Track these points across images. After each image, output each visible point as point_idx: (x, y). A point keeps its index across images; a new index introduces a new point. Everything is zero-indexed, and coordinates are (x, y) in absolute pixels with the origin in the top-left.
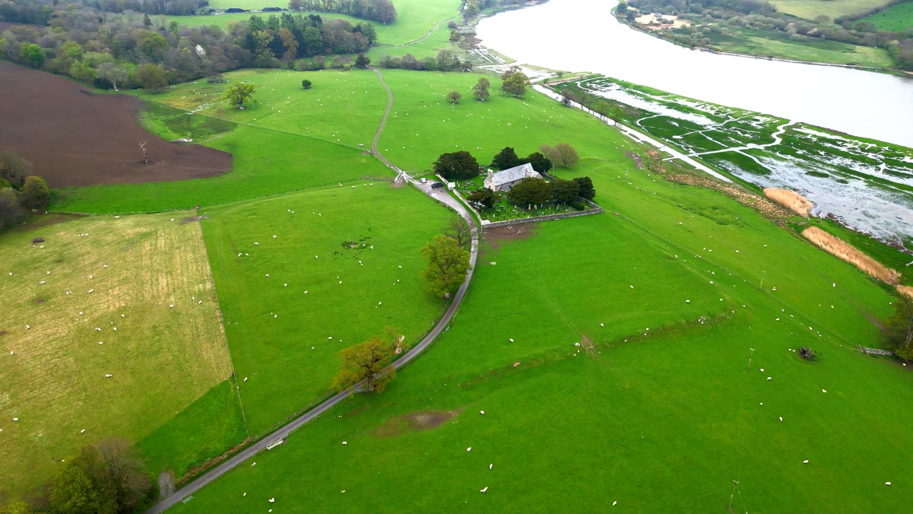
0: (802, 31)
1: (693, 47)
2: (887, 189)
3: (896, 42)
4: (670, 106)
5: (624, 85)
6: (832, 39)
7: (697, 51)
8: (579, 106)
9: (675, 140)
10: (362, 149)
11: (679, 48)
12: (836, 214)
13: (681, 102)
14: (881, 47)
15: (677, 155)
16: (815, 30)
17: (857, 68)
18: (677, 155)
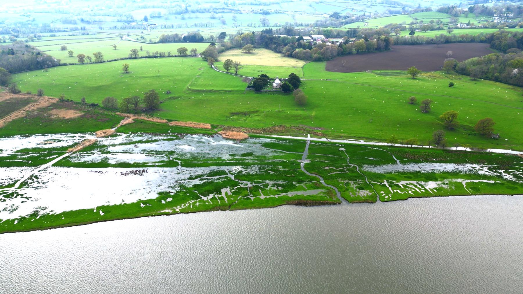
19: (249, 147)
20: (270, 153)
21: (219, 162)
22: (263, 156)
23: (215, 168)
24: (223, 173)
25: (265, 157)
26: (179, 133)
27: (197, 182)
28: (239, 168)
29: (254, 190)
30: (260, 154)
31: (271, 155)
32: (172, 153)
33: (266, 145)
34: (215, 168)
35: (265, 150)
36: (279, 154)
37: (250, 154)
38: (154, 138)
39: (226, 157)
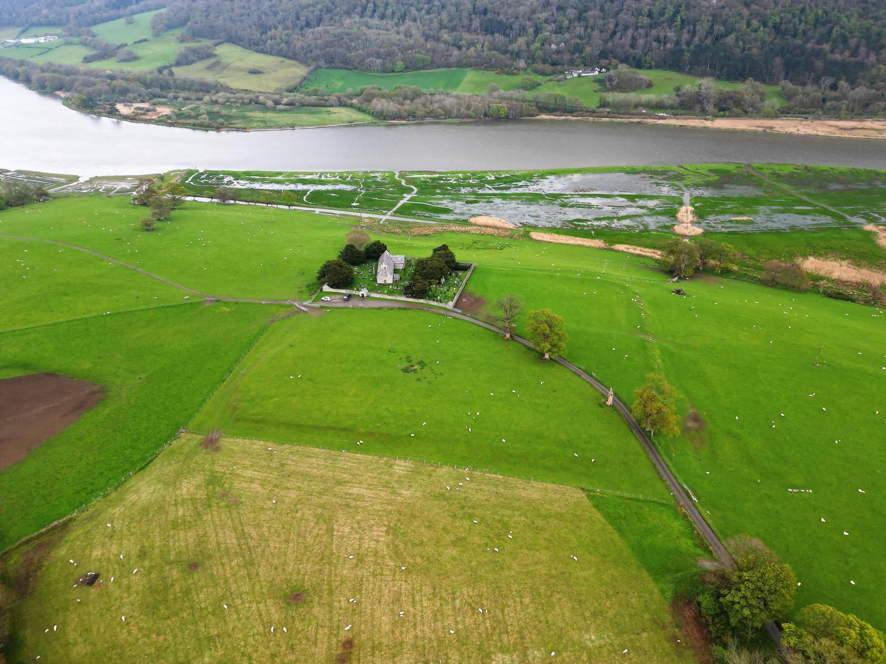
0: (277, 103)
1: (218, 129)
2: (513, 199)
3: (355, 101)
4: (304, 182)
5: (237, 176)
6: (304, 105)
7: (223, 133)
8: (232, 202)
9: (355, 207)
10: (190, 301)
11: (200, 134)
12: (524, 221)
13: (301, 177)
14: (346, 105)
15: (384, 218)
16: (285, 100)
17: (357, 125)
18: (384, 218)
19: (470, 210)
20: (446, 203)
21: (504, 197)
22: (453, 200)
23: (505, 192)
24: (496, 189)
25: (452, 199)
26: (574, 228)
27: (520, 184)
28: (480, 191)
29: (464, 179)
30: (458, 202)
31: (445, 202)
32: (564, 205)
33: (447, 211)
34: (505, 192)
35: (450, 206)
36: (435, 201)
37: (468, 202)
38: (604, 223)
39: (497, 201)
